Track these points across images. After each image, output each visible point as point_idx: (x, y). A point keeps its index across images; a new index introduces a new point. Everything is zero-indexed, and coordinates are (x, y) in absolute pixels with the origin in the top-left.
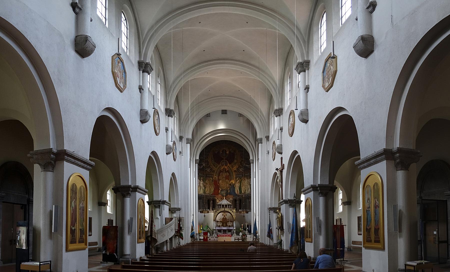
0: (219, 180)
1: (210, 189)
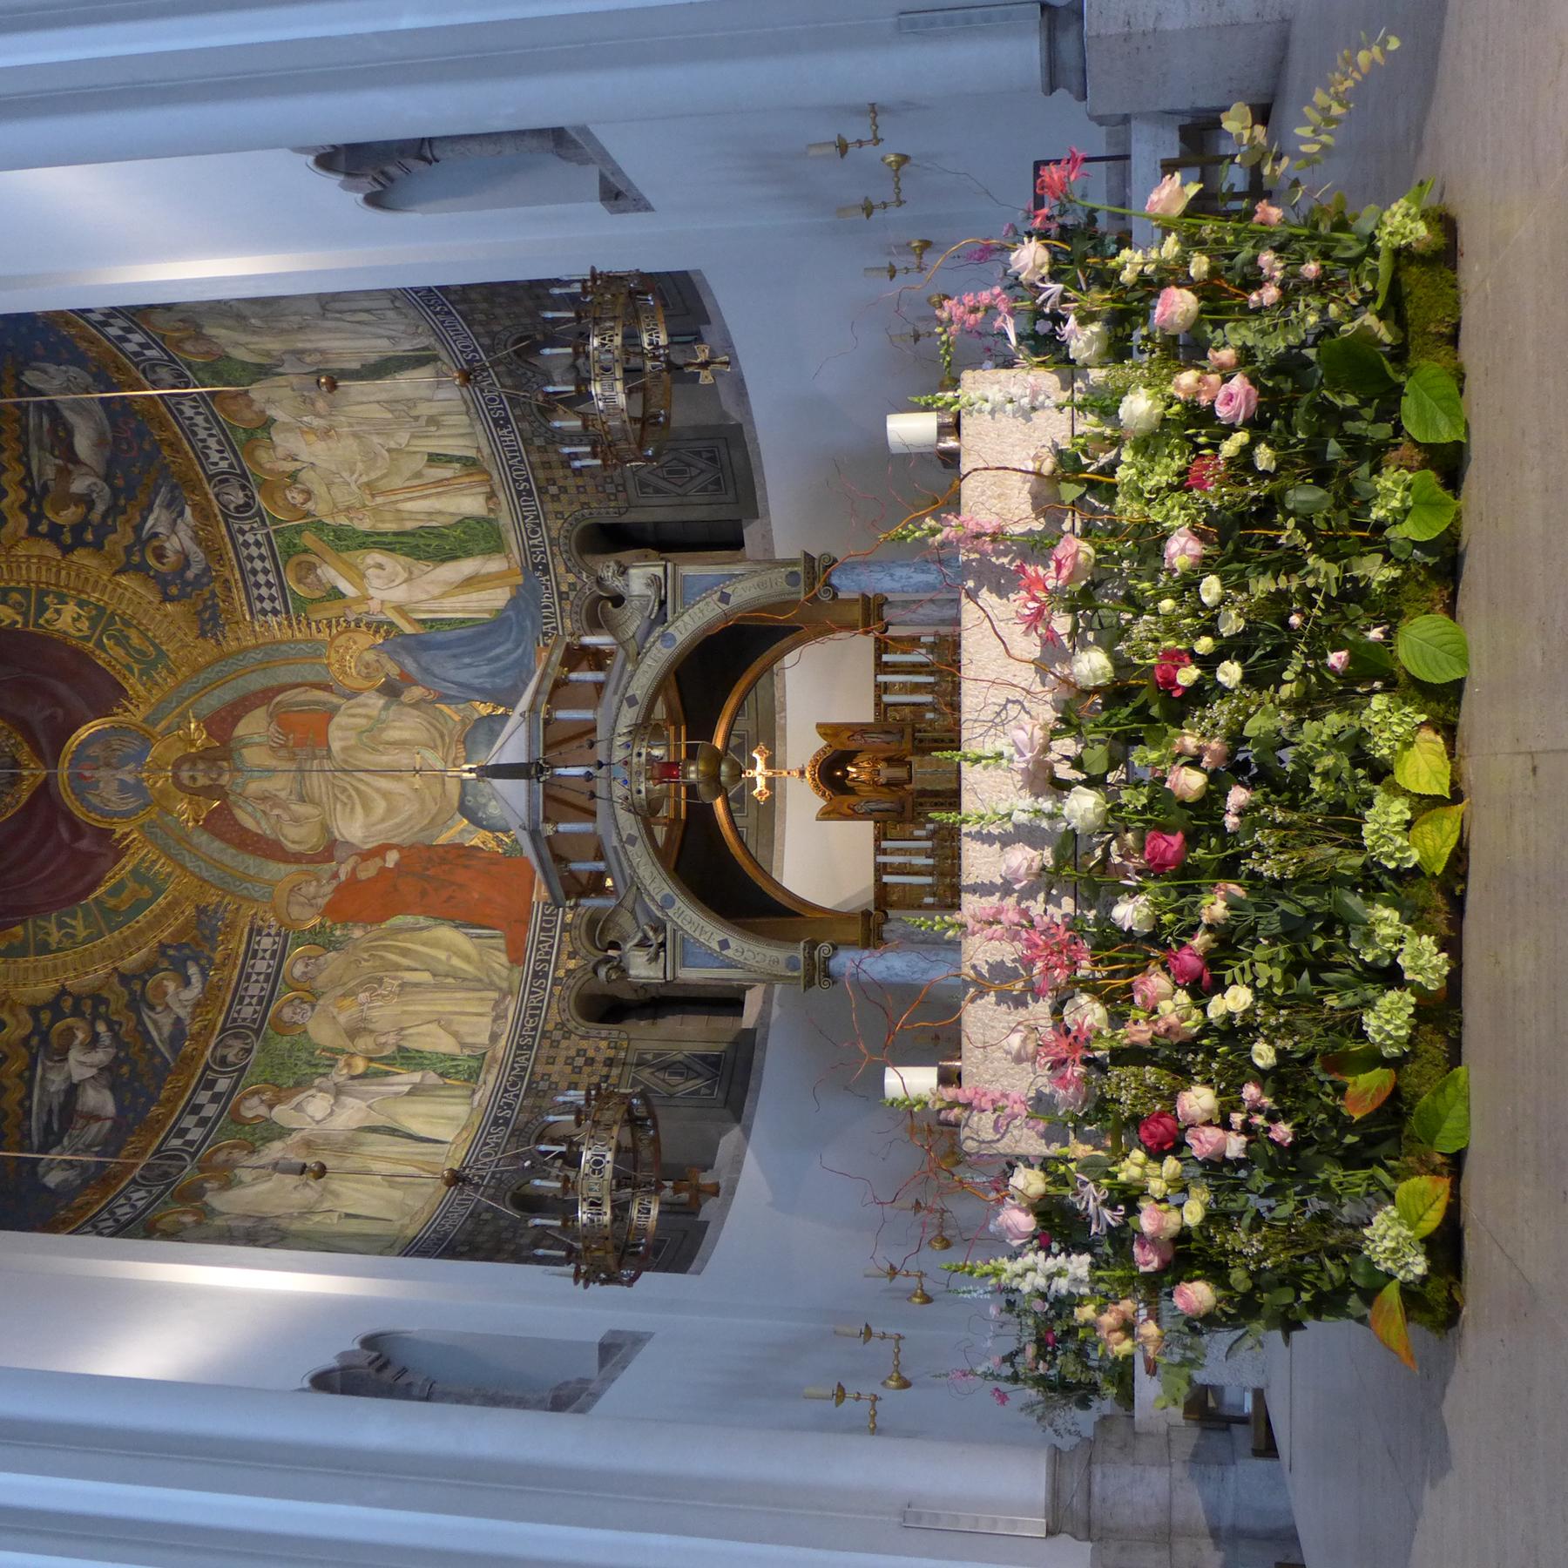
0: (330, 849)
1: (438, 987)
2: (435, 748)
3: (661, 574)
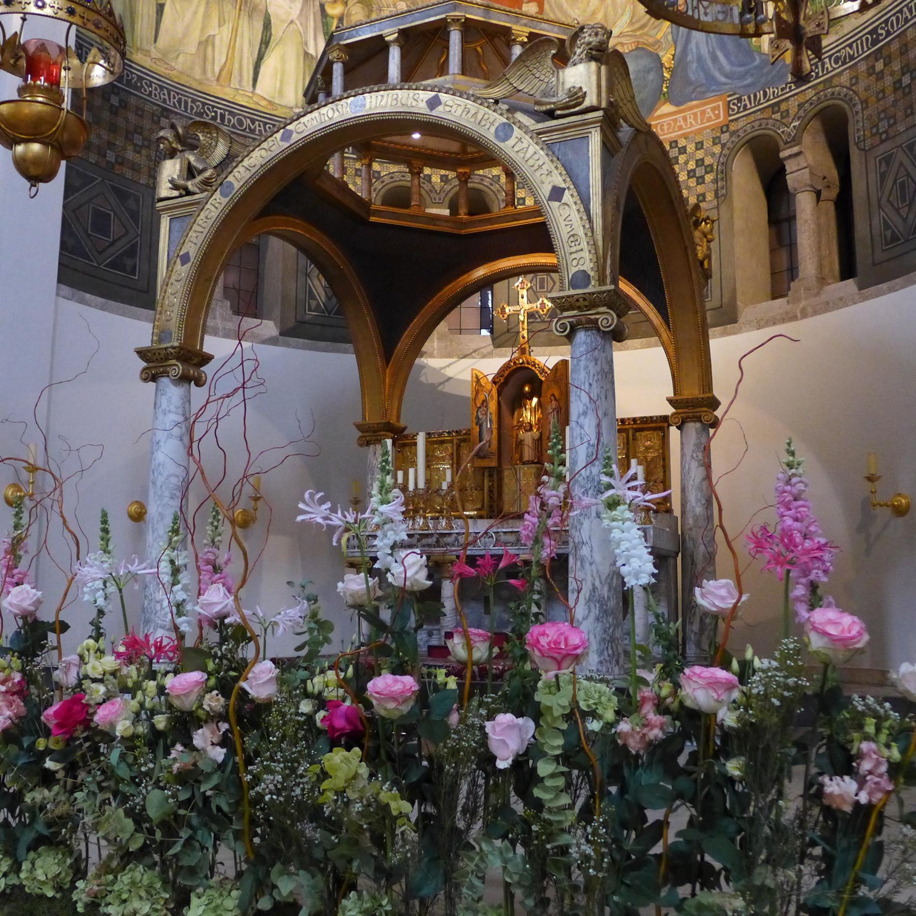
2: (631, 23)
3: (587, 103)
